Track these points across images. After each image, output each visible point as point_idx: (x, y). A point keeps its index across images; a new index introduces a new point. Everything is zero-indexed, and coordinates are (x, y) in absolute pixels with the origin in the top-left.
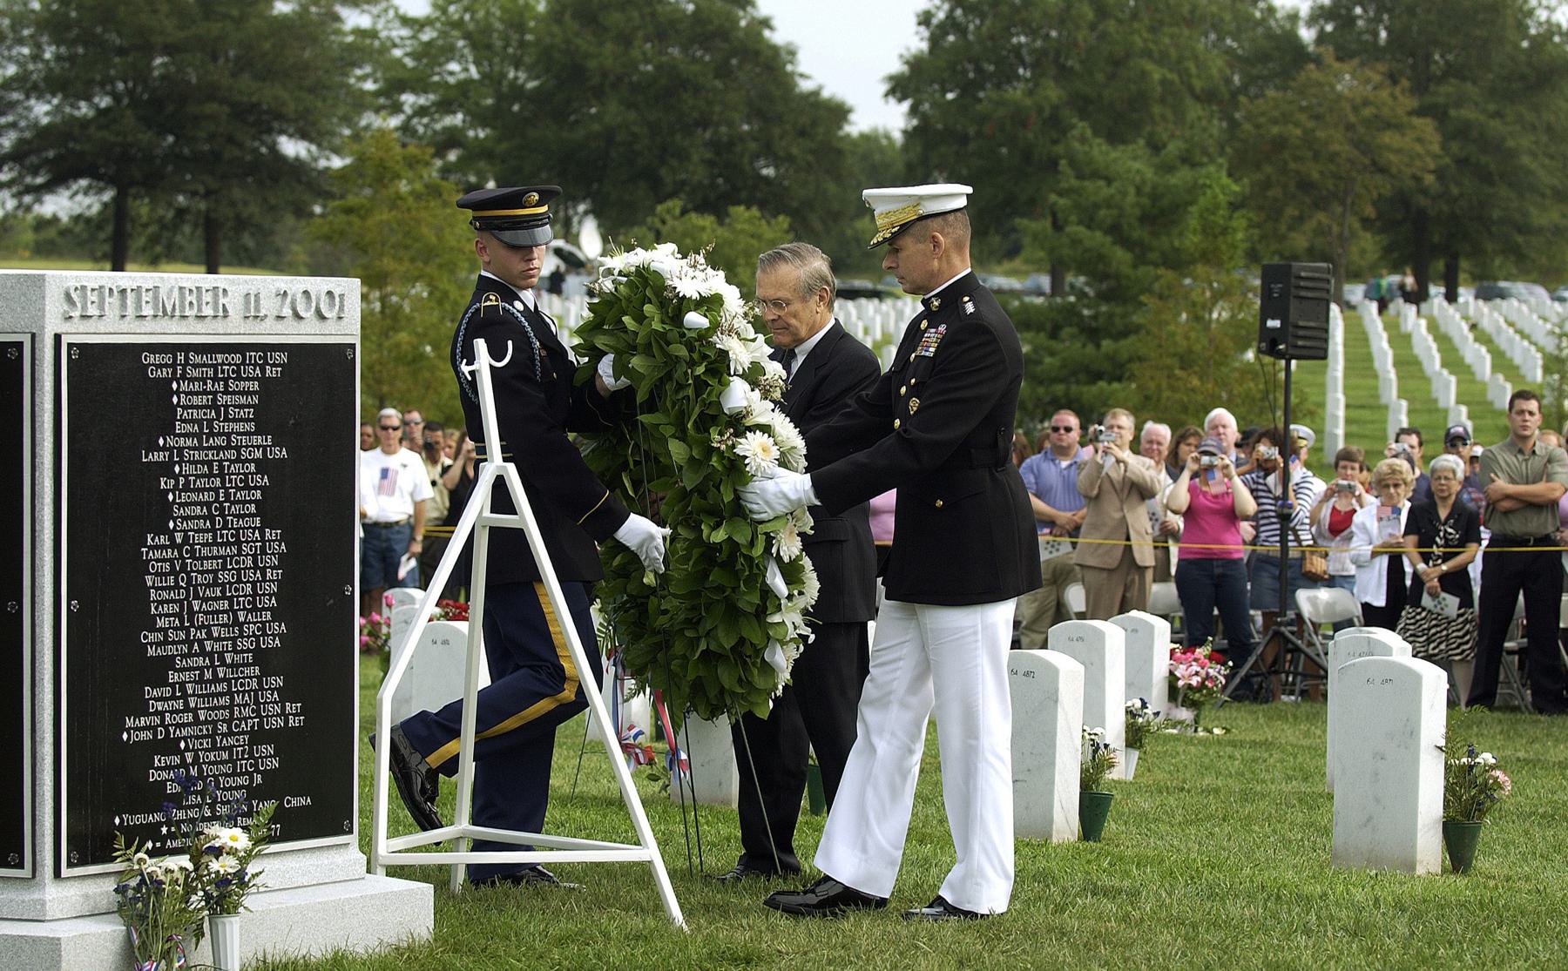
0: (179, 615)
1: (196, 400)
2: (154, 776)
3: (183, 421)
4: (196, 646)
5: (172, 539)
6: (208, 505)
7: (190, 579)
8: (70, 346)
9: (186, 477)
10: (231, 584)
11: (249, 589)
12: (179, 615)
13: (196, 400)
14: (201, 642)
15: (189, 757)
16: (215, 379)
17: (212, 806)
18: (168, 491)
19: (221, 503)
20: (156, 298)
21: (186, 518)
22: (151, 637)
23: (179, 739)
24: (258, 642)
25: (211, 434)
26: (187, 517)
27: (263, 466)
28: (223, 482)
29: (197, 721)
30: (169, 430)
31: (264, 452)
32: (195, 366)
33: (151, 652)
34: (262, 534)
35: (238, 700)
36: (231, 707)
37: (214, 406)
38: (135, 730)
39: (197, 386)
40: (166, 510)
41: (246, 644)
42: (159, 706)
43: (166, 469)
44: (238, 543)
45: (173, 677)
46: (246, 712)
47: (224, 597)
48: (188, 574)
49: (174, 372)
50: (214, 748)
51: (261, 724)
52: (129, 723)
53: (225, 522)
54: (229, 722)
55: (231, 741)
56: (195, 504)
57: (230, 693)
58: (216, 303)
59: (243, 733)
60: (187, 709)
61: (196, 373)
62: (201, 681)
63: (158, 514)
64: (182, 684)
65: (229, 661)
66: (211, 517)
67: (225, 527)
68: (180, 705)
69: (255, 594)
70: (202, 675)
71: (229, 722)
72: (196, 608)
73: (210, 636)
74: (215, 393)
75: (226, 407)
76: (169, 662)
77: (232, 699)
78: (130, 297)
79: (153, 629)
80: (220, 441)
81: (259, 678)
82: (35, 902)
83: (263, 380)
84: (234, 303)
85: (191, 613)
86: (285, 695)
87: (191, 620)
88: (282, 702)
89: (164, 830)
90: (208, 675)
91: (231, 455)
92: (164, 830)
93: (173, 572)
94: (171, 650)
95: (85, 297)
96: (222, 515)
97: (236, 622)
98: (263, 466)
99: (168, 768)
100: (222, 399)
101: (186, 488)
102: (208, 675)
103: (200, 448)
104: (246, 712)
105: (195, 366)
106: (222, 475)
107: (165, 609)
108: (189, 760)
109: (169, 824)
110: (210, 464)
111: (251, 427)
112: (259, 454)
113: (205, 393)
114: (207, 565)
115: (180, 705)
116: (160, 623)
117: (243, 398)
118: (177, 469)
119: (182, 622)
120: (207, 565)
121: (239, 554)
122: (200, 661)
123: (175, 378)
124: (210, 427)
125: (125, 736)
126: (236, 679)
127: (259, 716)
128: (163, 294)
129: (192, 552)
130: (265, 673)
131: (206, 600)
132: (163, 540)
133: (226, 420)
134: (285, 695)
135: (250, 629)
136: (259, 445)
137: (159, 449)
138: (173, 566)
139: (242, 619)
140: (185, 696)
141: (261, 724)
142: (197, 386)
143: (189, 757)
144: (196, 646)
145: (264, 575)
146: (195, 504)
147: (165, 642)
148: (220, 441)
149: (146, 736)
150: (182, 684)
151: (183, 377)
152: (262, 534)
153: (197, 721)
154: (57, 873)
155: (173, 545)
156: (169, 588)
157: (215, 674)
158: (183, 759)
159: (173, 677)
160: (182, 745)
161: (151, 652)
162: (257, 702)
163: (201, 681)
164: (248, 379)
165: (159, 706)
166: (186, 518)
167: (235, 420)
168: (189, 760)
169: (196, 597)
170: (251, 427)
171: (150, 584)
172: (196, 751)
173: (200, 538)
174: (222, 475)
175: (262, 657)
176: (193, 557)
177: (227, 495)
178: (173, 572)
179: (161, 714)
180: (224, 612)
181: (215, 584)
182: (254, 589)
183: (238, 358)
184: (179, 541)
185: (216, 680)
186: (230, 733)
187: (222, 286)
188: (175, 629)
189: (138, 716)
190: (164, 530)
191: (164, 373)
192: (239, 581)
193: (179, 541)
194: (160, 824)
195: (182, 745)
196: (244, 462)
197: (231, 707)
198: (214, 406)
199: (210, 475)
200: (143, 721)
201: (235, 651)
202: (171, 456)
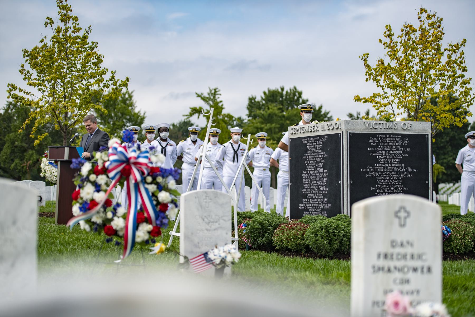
0: (309, 186)
1: (311, 147)
6: (314, 166)
12: (309, 186)
13: (311, 147)
21: (310, 168)
25: (314, 153)
26: (310, 168)
27: (323, 158)
29: (312, 206)
30: (307, 152)
36: (318, 204)
37: (314, 148)
39: (311, 144)
41: (320, 192)
43: (306, 160)
44: (319, 173)
45: (308, 197)
46: (321, 205)
50: (315, 211)
54: (318, 206)
57: (318, 201)
60: (310, 203)
62: (313, 198)
63: (305, 168)
64: (309, 199)
66: (314, 168)
68: (309, 203)
71: (318, 206)
79: (304, 188)
80: (315, 154)
83: (323, 142)
86: (328, 202)
90: (314, 197)
91: (317, 156)
93: (307, 178)
94: (307, 192)
97: (319, 188)
98: (323, 158)
100: (316, 146)
101: (310, 163)
102: (314, 197)
104: (321, 205)
107: (306, 185)
110: (314, 158)
114: (314, 177)
115: (309, 203)
116: (305, 187)
120: (314, 177)
122: (312, 195)
130: (324, 198)
132: (305, 172)
134: (328, 202)
135: (321, 189)
136: (323, 154)
140: (310, 201)
142: (311, 144)
143: (310, 212)
147: (306, 191)
148: (315, 154)
150: (309, 199)
153: (312, 206)
155: (307, 173)
159: (308, 197)
163: (313, 198)
166: (310, 168)
170: (321, 151)
173: (312, 172)
174: (316, 160)
179: (305, 204)
183: (318, 138)
186: (318, 209)
190: (306, 171)
191: (305, 142)
197: (318, 204)
198: (314, 148)
199: (314, 160)
200: (302, 205)
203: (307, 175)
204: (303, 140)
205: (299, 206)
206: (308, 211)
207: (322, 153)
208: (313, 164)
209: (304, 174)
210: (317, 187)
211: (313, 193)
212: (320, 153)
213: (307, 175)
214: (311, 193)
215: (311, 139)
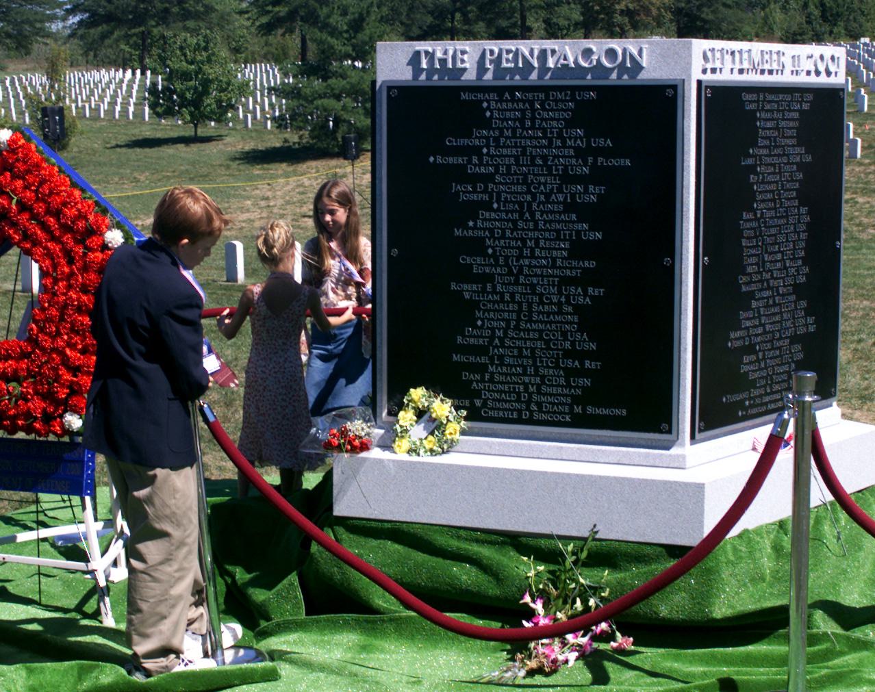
0: (757, 264)
2: (744, 369)
3: (762, 138)
4: (765, 284)
5: (755, 214)
7: (763, 240)
8: (707, 87)
9: (763, 174)
10: (783, 242)
11: (791, 245)
12: (757, 264)
14: (768, 281)
15: (760, 354)
16: (778, 111)
17: (771, 386)
18: (753, 184)
19: (779, 191)
20: (749, 57)
21: (763, 201)
22: (745, 279)
23: (755, 345)
24: (795, 279)
25: (776, 147)
27: (801, 166)
28: (781, 178)
30: (754, 144)
31: (801, 158)
32: (769, 102)
33: (744, 289)
34: (799, 210)
35: (785, 316)
37: (777, 128)
38: (735, 339)
40: (752, 196)
42: (748, 323)
43: (752, 169)
47: (780, 252)
48: (762, 237)
49: (758, 106)
50: (773, 349)
51: (795, 331)
52: (732, 336)
53: (781, 203)
55: (781, 343)
56: (766, 191)
58: (779, 61)
59: (786, 338)
61: (768, 107)
62: (767, 306)
65: (781, 292)
66: (773, 200)
67: (781, 207)
69: (795, 249)
70: (768, 302)
72: (766, 259)
73: (772, 277)
74: (777, 120)
75: (783, 128)
76: (751, 296)
77: (782, 317)
78: (737, 55)
79: (745, 274)
80: (779, 151)
81: (795, 302)
82: (678, 456)
84: (787, 60)
85: (764, 262)
86: (808, 312)
87: (763, 267)
88: (807, 315)
89: (747, 403)
92: (747, 403)
93: (756, 237)
94: (753, 287)
95: (714, 55)
96: (780, 199)
97: (785, 268)
99: (750, 363)
102: (771, 302)
103: (770, 156)
104: (789, 324)
105: (769, 102)
106: (780, 173)
108: (761, 357)
109: (750, 399)
111: (794, 141)
112: (798, 159)
113: (773, 119)
116: (749, 270)
117: (790, 125)
118: (759, 169)
119: (759, 269)
121: (788, 224)
123: (758, 110)
124: (775, 142)
125: (730, 344)
126: (784, 304)
127: (795, 326)
128: (753, 53)
129: (765, 222)
130: (799, 299)
131: (771, 253)
132: (751, 216)
133: (784, 137)
134: (808, 312)
137: (750, 156)
138: (755, 233)
139: (788, 265)
140: (760, 316)
141: (795, 331)
142: (769, 115)
144: (765, 284)
145: (799, 236)
146: (766, 191)
147: (751, 282)
148: (779, 151)
149: (739, 343)
151: (763, 109)
152: (799, 210)
153: (765, 332)
154: (693, 437)
155: (757, 219)
156: (753, 247)
157: (774, 301)
158: (758, 357)
159: (754, 304)
160: (758, 348)
161: (744, 289)
162: (794, 318)
164: (794, 111)
165: (748, 323)
166: (763, 201)
167: (787, 137)
168: (761, 357)
169: (766, 252)
170: (794, 141)
171: (744, 244)
172: (764, 351)
175: (796, 287)
176: (765, 227)
177: (782, 185)
178: (756, 237)
179: (747, 328)
180: (779, 261)
181: (776, 243)
182: (794, 246)
184: (759, 216)
185: (775, 305)
187: (782, 50)
188: (756, 273)
189: (736, 331)
191: (753, 106)
192: (787, 241)
193: (759, 216)
194: (745, 399)
195: (758, 348)
196: (791, 164)
199: (774, 173)
201: (784, 286)
202: (756, 161)
203: (755, 224)
204: (749, 97)
205: (728, 339)
206: (756, 353)
207: (798, 150)
208: (773, 187)
209: (747, 221)
210: (779, 265)
211: (769, 288)
212: (791, 151)
213: (755, 224)
214: (761, 290)
215: (770, 97)
